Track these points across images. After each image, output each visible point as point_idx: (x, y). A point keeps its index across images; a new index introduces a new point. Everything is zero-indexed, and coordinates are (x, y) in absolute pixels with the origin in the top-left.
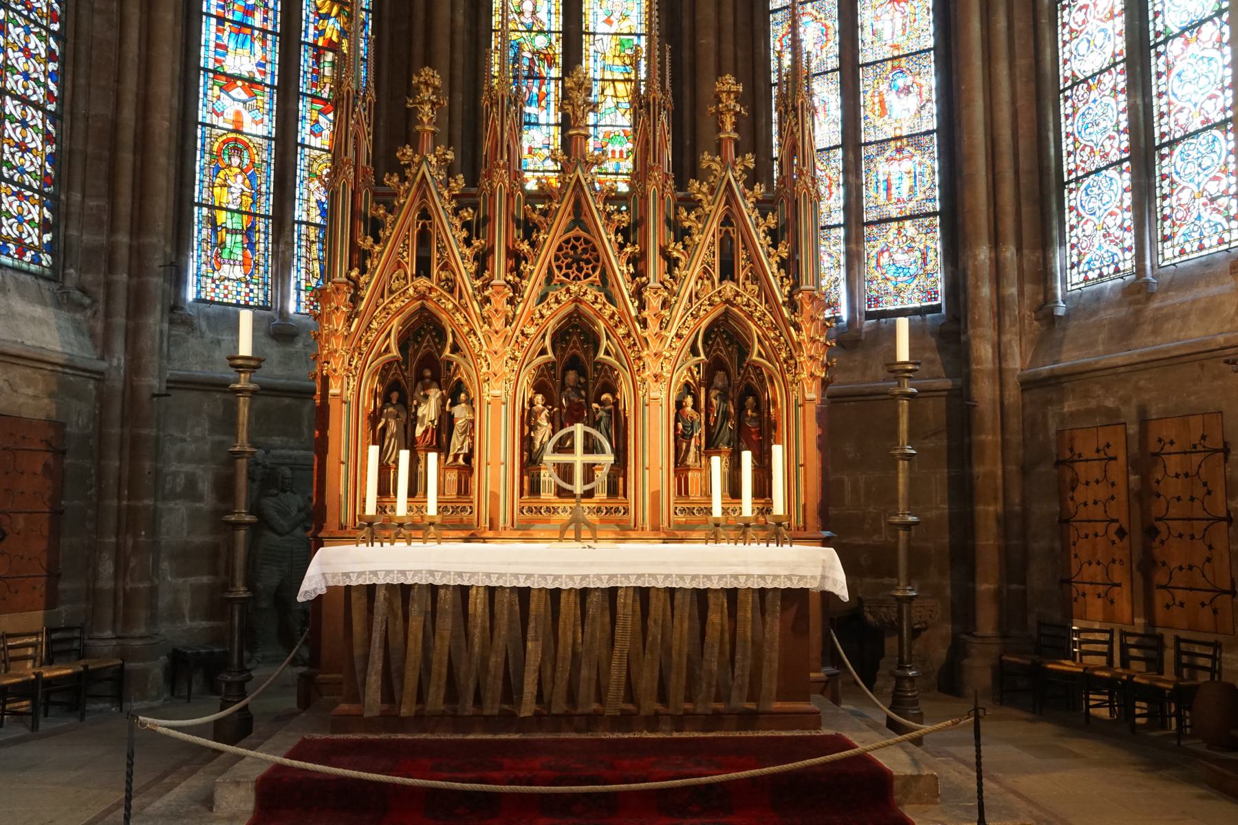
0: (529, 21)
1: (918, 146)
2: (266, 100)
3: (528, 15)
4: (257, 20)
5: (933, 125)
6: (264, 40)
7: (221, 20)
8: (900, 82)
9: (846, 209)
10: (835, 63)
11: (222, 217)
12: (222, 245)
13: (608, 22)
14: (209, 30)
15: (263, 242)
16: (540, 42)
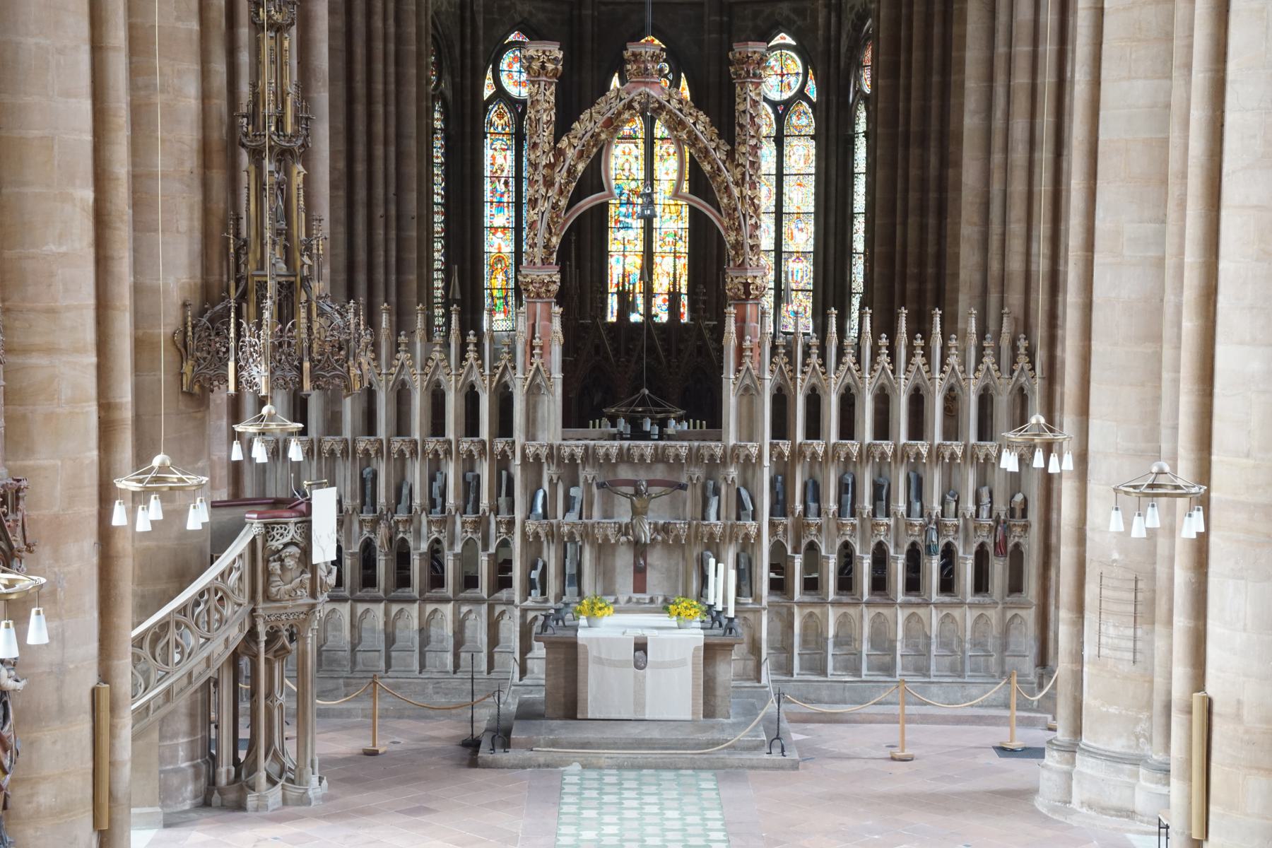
0: (627, 173)
1: (805, 257)
2: (510, 235)
3: (627, 171)
4: (505, 199)
5: (812, 249)
6: (508, 207)
7: (492, 203)
8: (800, 226)
9: (775, 281)
10: (773, 209)
11: (495, 293)
12: (496, 305)
13: (667, 174)
14: (487, 210)
15: (511, 301)
16: (633, 185)
